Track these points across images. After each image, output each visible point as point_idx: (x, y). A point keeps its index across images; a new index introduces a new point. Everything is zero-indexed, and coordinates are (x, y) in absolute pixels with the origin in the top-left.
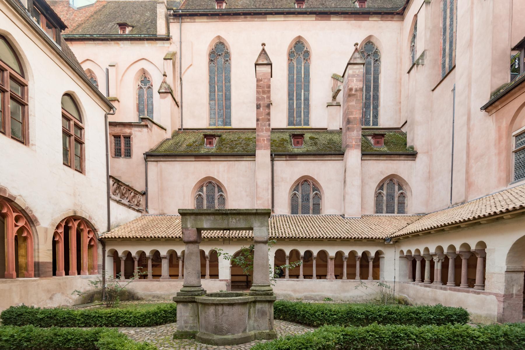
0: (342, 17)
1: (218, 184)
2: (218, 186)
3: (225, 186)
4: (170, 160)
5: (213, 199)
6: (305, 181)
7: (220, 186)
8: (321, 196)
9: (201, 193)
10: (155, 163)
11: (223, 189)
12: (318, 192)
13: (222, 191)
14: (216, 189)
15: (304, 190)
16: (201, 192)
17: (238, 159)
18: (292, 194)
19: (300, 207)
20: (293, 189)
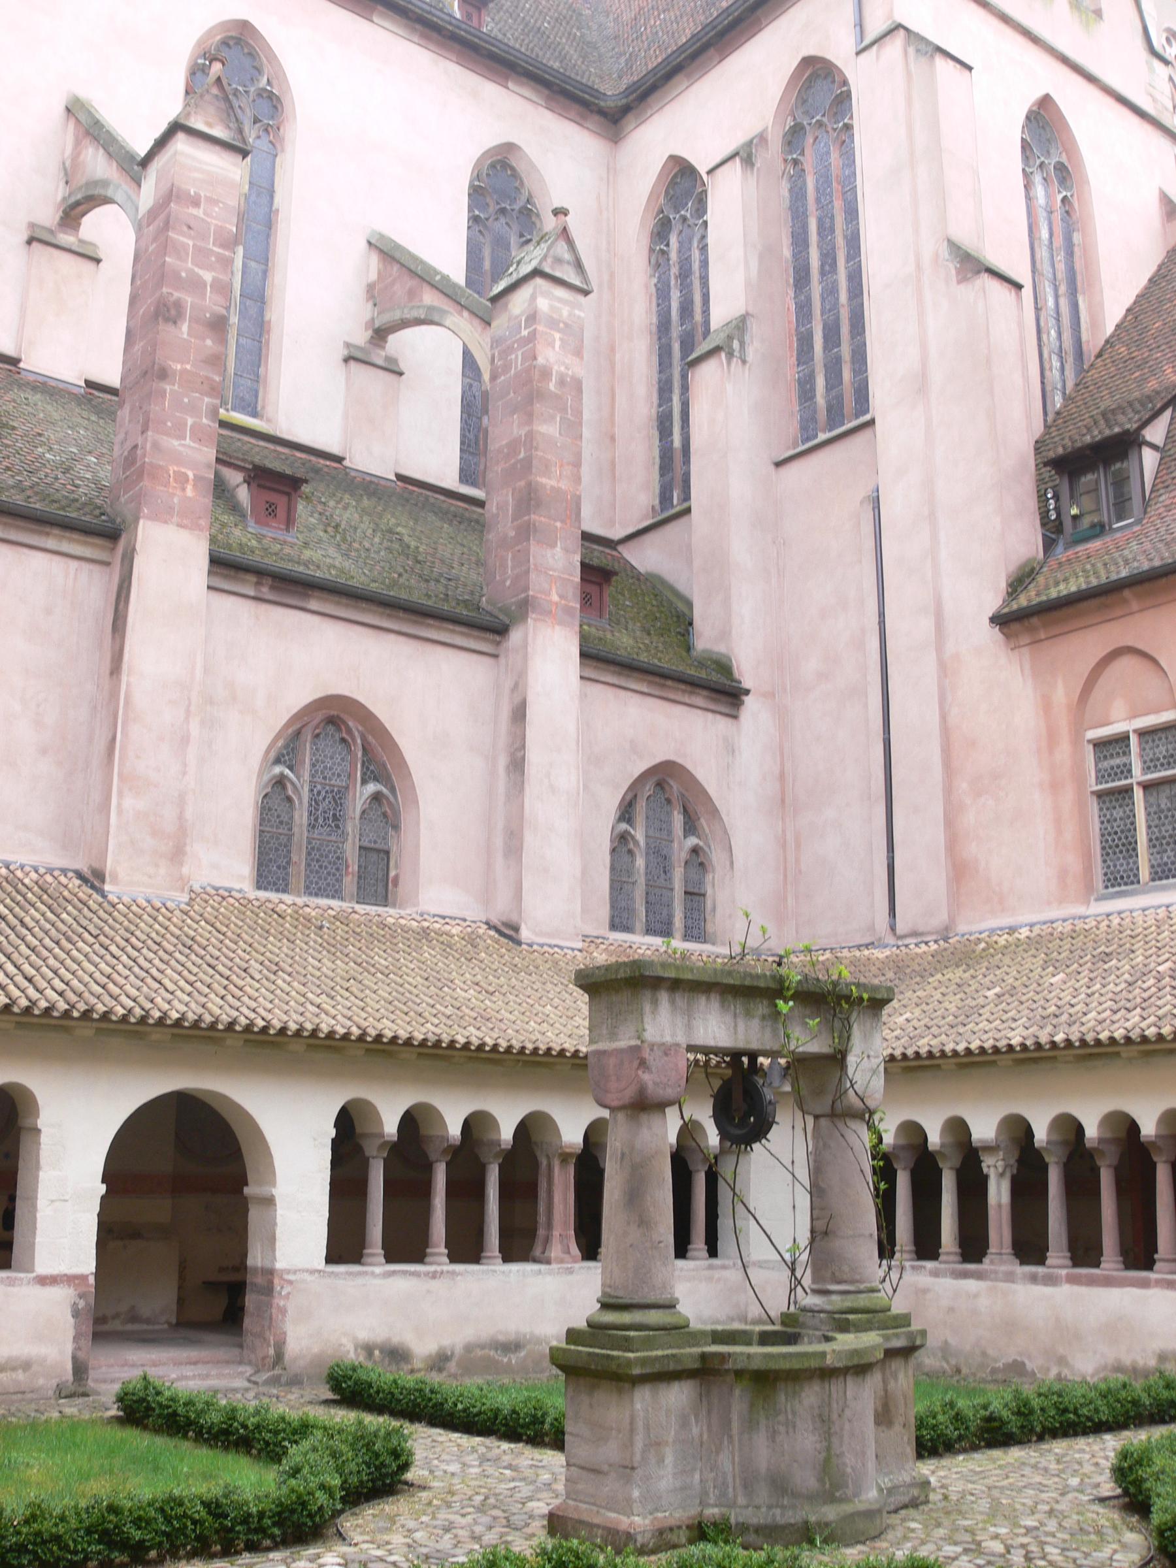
6: (333, 721)
8: (396, 813)
12: (385, 791)
15: (320, 767)
18: (266, 778)
19: (299, 857)
20: (272, 755)
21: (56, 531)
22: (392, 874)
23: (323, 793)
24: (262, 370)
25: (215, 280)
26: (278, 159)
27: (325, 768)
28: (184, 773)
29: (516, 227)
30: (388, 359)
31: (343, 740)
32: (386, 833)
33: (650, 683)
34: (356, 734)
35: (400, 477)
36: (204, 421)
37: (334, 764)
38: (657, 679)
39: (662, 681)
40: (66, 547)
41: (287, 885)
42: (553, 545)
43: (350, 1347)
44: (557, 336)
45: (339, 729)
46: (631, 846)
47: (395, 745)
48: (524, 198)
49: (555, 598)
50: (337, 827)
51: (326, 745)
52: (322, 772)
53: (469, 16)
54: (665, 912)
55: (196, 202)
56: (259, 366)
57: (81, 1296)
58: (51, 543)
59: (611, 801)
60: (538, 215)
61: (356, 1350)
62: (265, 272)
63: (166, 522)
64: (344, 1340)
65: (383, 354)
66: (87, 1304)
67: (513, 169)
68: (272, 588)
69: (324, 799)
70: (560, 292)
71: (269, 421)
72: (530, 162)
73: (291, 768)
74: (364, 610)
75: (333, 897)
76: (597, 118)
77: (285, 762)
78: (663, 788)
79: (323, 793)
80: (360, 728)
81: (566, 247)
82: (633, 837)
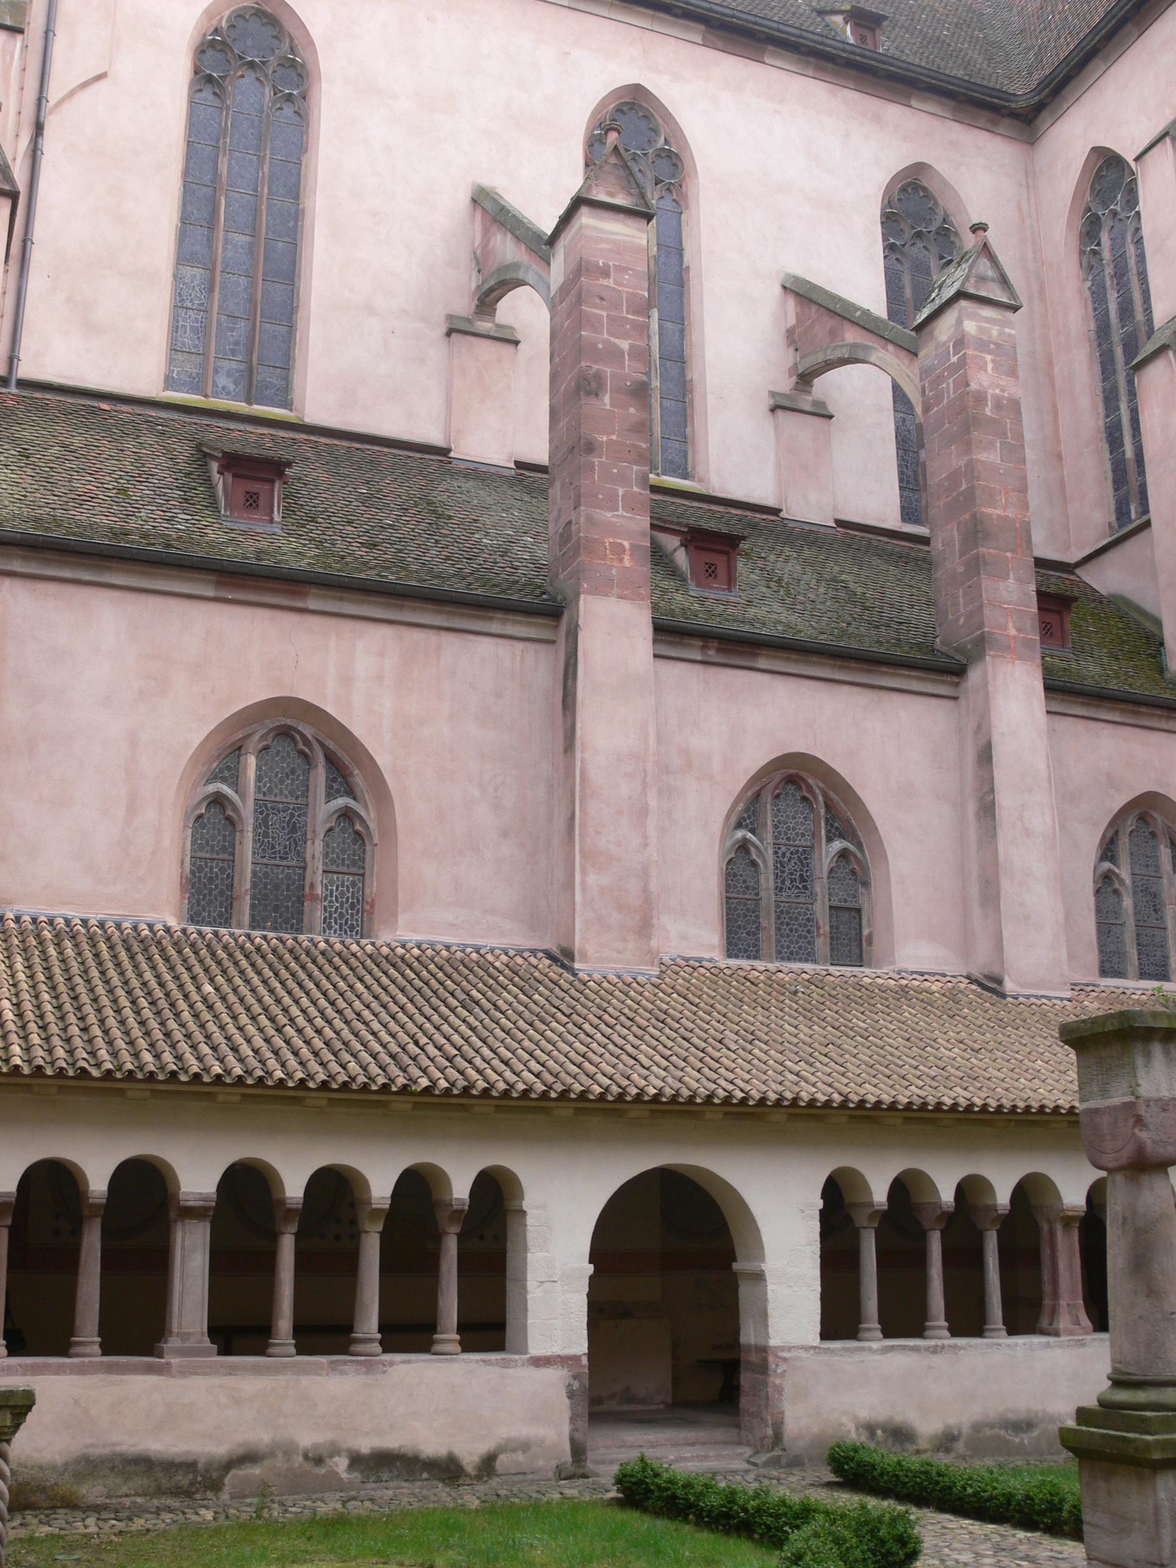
0: (808, 63)
1: (331, 745)
2: (332, 761)
3: (380, 761)
5: (296, 832)
6: (792, 780)
7: (346, 759)
8: (865, 870)
11: (358, 779)
12: (851, 847)
13: (351, 792)
14: (320, 775)
15: (781, 829)
16: (224, 780)
18: (729, 843)
19: (768, 922)
20: (733, 820)
21: (499, 615)
22: (865, 932)
23: (788, 854)
24: (688, 430)
25: (631, 347)
26: (683, 216)
27: (788, 828)
28: (646, 845)
29: (934, 250)
30: (816, 403)
31: (804, 799)
32: (856, 891)
33: (1122, 711)
34: (817, 791)
35: (840, 523)
36: (635, 489)
37: (797, 823)
38: (1130, 707)
39: (1136, 709)
40: (510, 630)
41: (757, 951)
42: (1006, 578)
43: (851, 1427)
44: (989, 358)
45: (799, 788)
46: (1117, 886)
47: (859, 799)
48: (939, 218)
49: (1013, 632)
50: (805, 888)
51: (787, 805)
52: (786, 834)
53: (863, 39)
54: (1159, 953)
55: (605, 273)
56: (686, 427)
57: (575, 1377)
58: (495, 627)
59: (1090, 840)
60: (956, 234)
61: (857, 1429)
62: (682, 331)
63: (606, 595)
64: (844, 1420)
65: (811, 398)
66: (582, 1385)
67: (925, 189)
68: (719, 650)
69: (789, 860)
70: (988, 312)
71: (701, 481)
72: (945, 182)
73: (753, 831)
74: (814, 663)
75: (806, 961)
76: (1008, 121)
77: (746, 826)
78: (1146, 822)
79: (788, 854)
80: (821, 785)
81: (988, 263)
82: (1117, 876)
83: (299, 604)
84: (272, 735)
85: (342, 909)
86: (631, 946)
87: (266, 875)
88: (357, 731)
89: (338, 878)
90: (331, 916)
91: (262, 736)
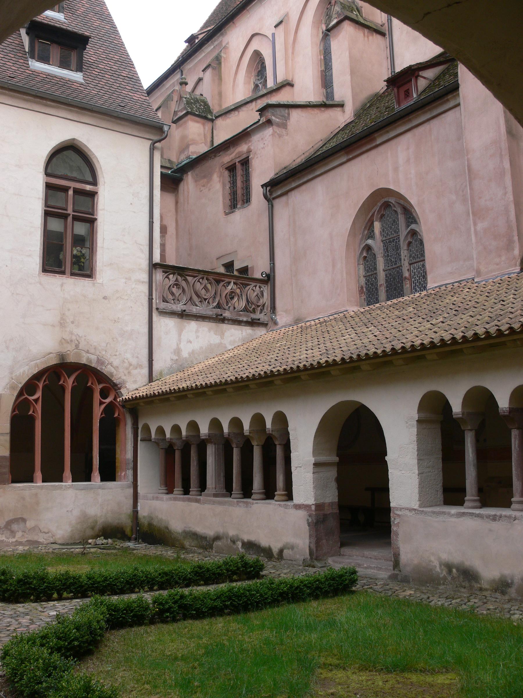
4: (305, 179)
9: (370, 242)
10: (284, 199)
17: (435, 113)
28: (506, 193)
43: (436, 563)
61: (440, 565)
64: (432, 558)
83: (374, 144)
84: (383, 209)
85: (420, 280)
86: (503, 258)
87: (390, 274)
88: (402, 192)
89: (417, 265)
90: (416, 285)
91: (378, 211)
